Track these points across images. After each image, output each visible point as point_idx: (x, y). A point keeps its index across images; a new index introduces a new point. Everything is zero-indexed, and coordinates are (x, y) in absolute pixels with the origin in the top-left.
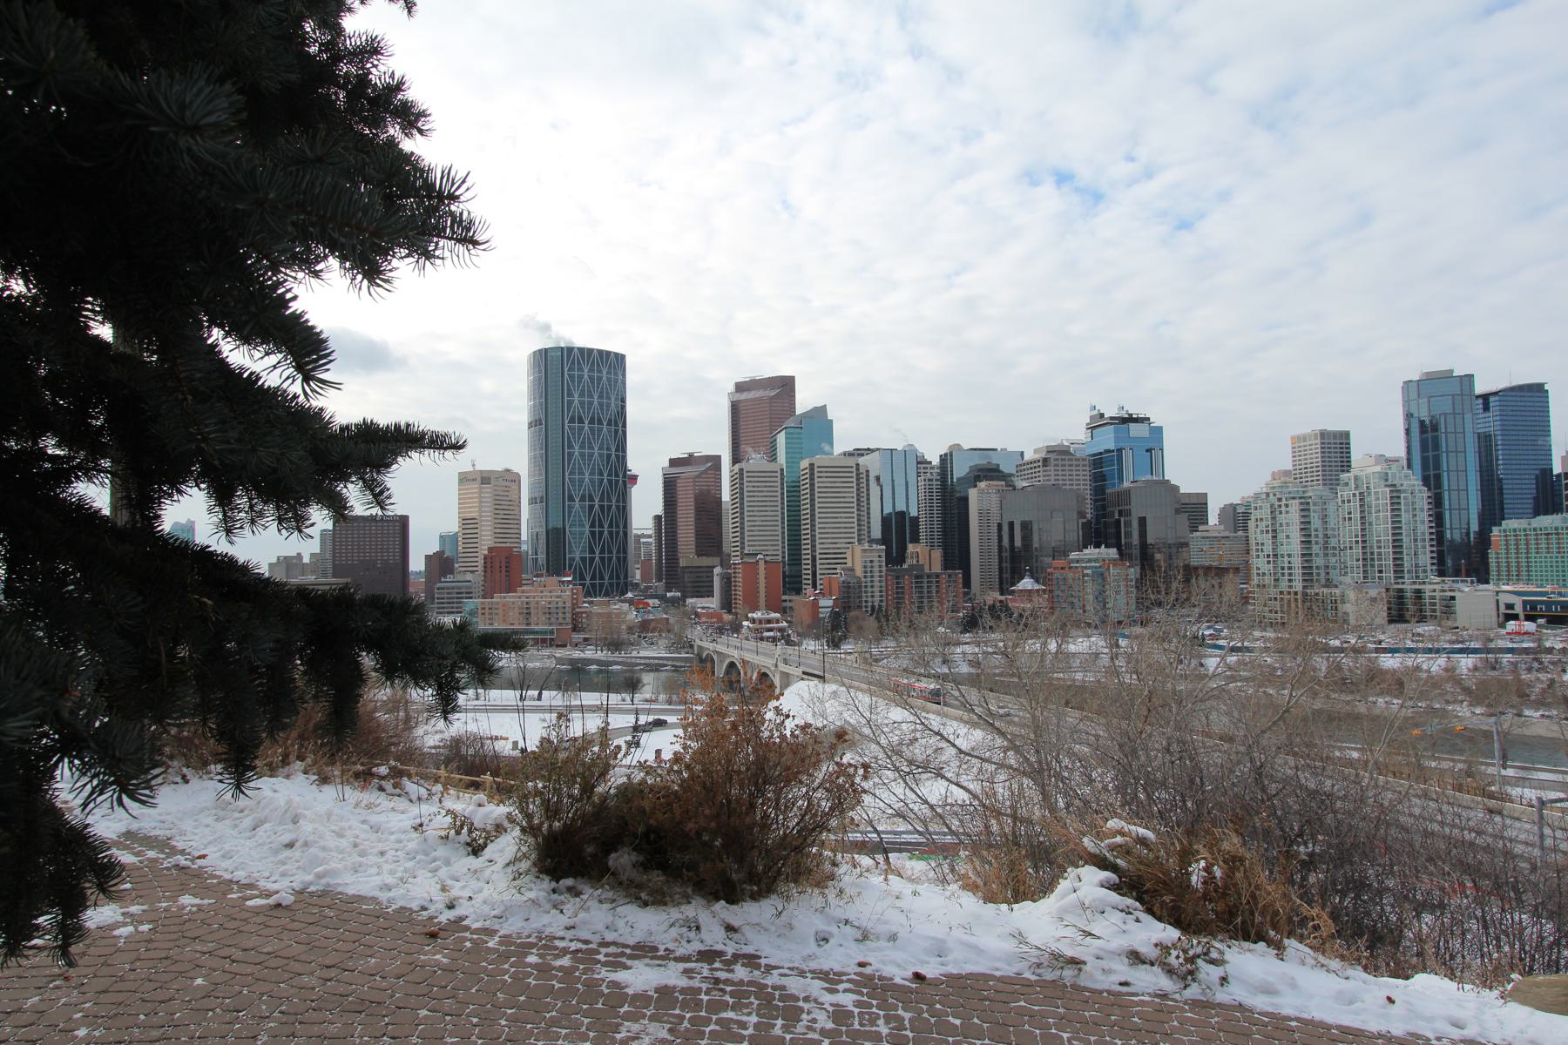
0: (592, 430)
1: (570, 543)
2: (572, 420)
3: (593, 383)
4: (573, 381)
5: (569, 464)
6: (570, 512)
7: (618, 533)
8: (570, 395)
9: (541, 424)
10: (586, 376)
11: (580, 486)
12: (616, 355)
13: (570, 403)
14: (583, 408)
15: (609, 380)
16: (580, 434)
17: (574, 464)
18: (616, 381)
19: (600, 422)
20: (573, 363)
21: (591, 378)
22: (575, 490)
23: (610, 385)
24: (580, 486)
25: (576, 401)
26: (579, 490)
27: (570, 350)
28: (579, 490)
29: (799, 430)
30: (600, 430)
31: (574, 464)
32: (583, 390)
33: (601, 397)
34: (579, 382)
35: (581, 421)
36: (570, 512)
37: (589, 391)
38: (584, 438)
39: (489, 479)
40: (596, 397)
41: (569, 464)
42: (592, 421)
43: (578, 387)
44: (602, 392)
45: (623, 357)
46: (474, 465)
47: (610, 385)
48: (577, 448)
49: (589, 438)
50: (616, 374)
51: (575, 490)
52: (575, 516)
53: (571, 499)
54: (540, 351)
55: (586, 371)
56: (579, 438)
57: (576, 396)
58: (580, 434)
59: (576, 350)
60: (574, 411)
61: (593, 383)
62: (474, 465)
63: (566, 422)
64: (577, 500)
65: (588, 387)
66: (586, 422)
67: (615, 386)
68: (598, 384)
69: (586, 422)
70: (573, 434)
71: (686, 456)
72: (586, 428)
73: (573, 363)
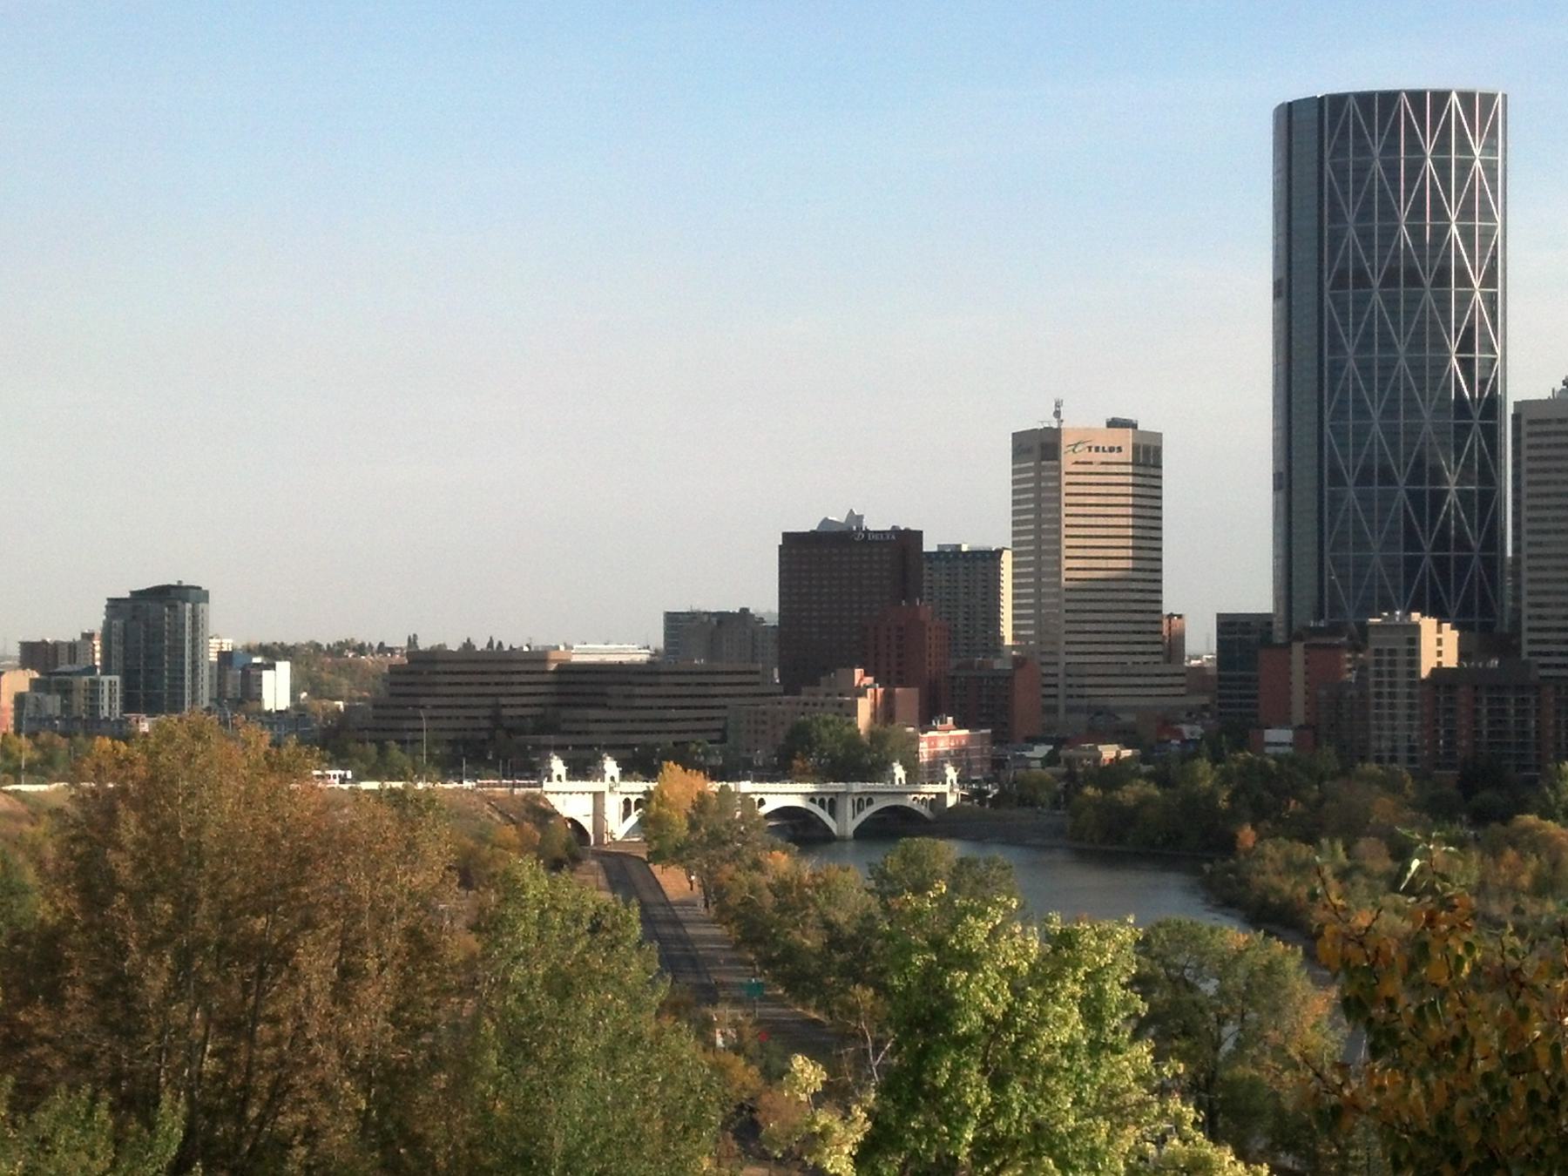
2: (1340, 281)
5: (1332, 391)
13: (1337, 237)
22: (1345, 457)
24: (1358, 445)
26: (1356, 456)
27: (1338, 101)
35: (1362, 279)
46: (1057, 414)
51: (1345, 457)
54: (1282, 105)
59: (1352, 100)
60: (1345, 258)
62: (1057, 414)
63: (1327, 285)
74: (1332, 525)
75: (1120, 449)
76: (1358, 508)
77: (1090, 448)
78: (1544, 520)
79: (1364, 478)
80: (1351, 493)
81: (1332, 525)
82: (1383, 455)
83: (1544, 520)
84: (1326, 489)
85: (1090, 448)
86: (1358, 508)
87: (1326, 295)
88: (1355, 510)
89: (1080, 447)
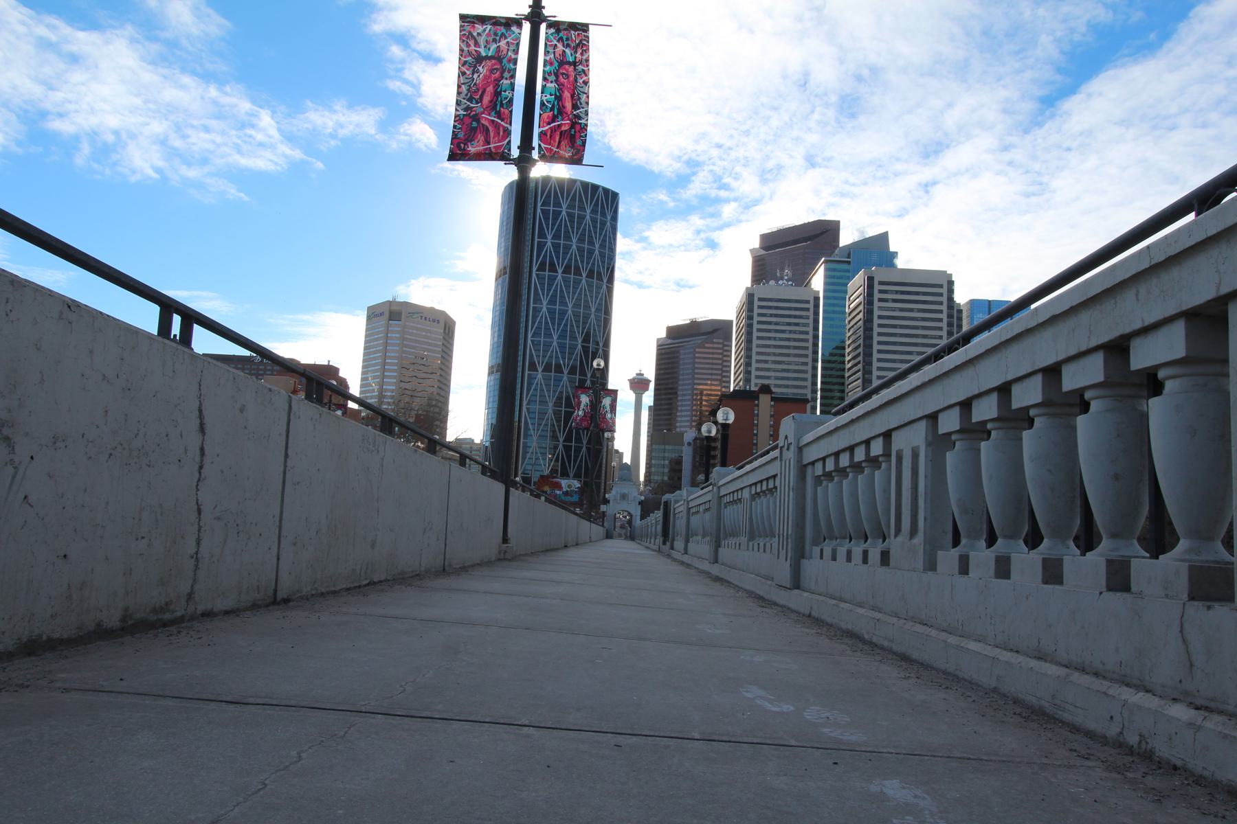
0: (566, 281)
1: (526, 423)
2: (541, 268)
3: (572, 222)
4: (547, 218)
5: (533, 323)
6: (530, 384)
8: (542, 235)
10: (564, 213)
11: (545, 351)
12: (606, 191)
13: (541, 246)
14: (557, 252)
15: (594, 221)
16: (550, 285)
17: (540, 323)
18: (603, 224)
19: (578, 273)
21: (571, 216)
23: (595, 227)
24: (545, 351)
25: (549, 244)
26: (544, 356)
28: (544, 356)
29: (845, 266)
30: (577, 283)
32: (559, 230)
33: (581, 240)
34: (555, 219)
35: (553, 268)
36: (530, 384)
37: (567, 232)
38: (556, 291)
39: (400, 314)
41: (533, 323)
42: (567, 270)
43: (553, 225)
44: (583, 234)
45: (615, 196)
47: (595, 227)
48: (545, 303)
49: (562, 291)
50: (603, 214)
51: (538, 356)
52: (535, 390)
55: (564, 207)
56: (549, 290)
58: (550, 285)
61: (572, 222)
63: (535, 269)
64: (540, 370)
65: (566, 226)
66: (560, 271)
67: (601, 229)
68: (579, 224)
69: (560, 271)
70: (542, 284)
71: (689, 322)
72: (559, 277)
75: (438, 322)
77: (422, 317)
78: (766, 362)
79: (547, 368)
82: (557, 357)
83: (766, 362)
85: (422, 317)
87: (534, 275)
88: (541, 384)
89: (416, 315)
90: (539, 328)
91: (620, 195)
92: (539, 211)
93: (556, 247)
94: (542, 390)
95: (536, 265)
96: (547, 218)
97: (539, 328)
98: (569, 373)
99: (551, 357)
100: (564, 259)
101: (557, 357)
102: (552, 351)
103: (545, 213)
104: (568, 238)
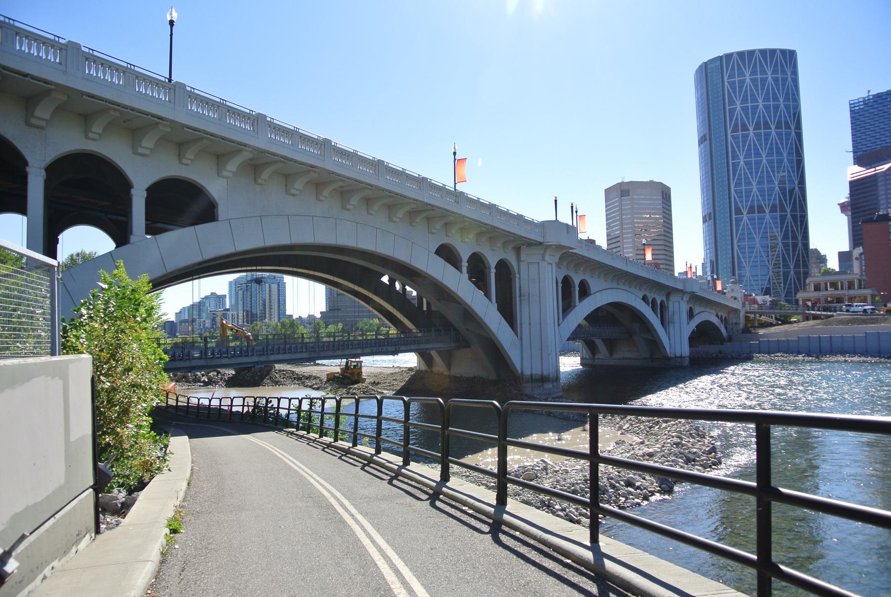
2: (735, 130)
5: (734, 175)
6: (737, 226)
7: (795, 246)
8: (732, 102)
9: (705, 140)
11: (747, 197)
12: (783, 52)
13: (732, 111)
17: (740, 174)
18: (785, 80)
19: (767, 126)
20: (733, 69)
22: (742, 202)
24: (747, 197)
26: (747, 201)
27: (729, 56)
28: (747, 201)
30: (768, 135)
31: (740, 174)
32: (746, 96)
35: (745, 128)
36: (737, 226)
40: (760, 101)
41: (734, 175)
48: (742, 157)
50: (784, 72)
51: (742, 202)
53: (738, 211)
57: (738, 103)
63: (729, 132)
64: (745, 212)
70: (737, 143)
73: (733, 69)
74: (737, 231)
76: (749, 223)
79: (751, 211)
80: (745, 217)
81: (737, 231)
82: (758, 200)
84: (734, 217)
86: (749, 223)
90: (740, 179)
91: (797, 51)
92: (726, 84)
93: (745, 109)
94: (748, 229)
95: (730, 127)
96: (734, 89)
97: (740, 179)
98: (770, 212)
99: (753, 200)
100: (753, 118)
101: (758, 200)
102: (753, 196)
103: (732, 84)
104: (754, 100)
